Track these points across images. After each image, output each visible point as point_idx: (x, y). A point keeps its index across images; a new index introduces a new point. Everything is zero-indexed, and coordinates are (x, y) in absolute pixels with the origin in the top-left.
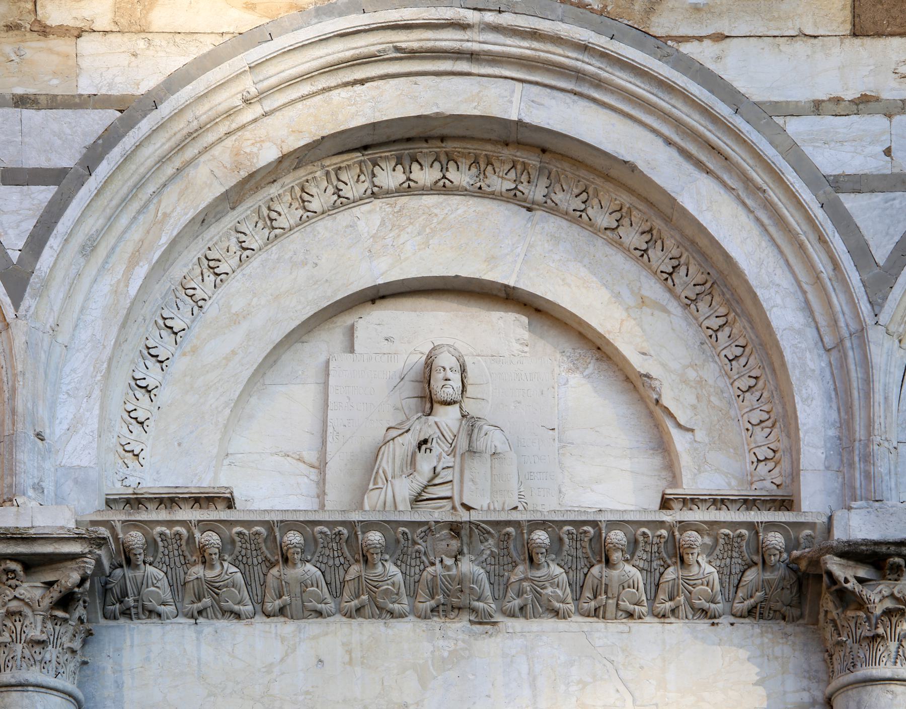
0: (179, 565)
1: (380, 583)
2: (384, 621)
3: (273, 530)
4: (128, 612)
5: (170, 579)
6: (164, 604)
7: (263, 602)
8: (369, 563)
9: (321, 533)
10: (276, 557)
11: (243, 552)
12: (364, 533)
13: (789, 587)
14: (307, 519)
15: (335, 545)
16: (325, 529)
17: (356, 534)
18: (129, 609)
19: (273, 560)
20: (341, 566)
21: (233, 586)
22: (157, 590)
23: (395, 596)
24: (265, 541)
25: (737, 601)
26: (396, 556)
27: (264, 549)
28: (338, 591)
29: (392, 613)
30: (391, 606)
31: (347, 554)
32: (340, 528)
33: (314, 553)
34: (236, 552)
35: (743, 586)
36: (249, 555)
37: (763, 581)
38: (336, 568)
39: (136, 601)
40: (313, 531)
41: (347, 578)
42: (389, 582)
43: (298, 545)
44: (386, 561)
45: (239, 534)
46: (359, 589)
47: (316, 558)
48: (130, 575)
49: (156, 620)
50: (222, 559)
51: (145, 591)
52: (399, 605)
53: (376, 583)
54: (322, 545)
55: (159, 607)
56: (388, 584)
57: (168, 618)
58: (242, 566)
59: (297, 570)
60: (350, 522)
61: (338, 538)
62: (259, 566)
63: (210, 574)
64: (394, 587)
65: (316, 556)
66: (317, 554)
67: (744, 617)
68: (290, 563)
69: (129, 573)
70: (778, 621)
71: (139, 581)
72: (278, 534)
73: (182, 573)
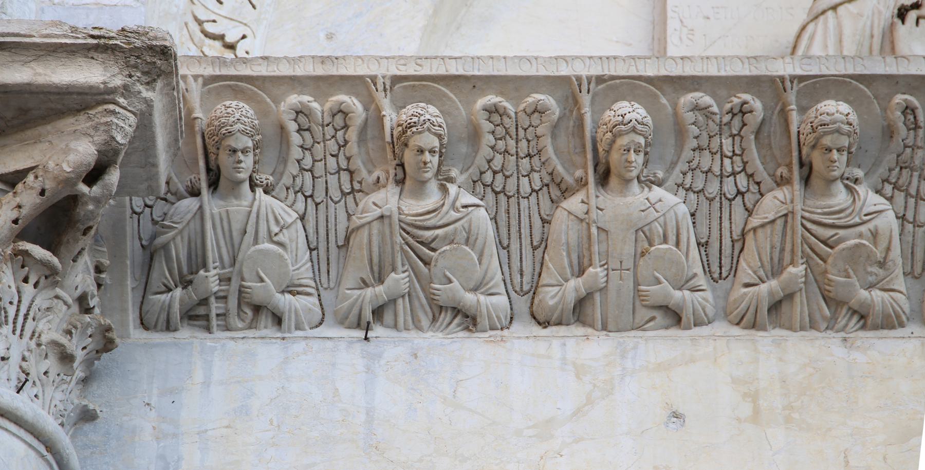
0: (336, 195)
1: (842, 232)
2: (843, 334)
3: (576, 102)
4: (201, 311)
5: (311, 231)
6: (292, 289)
7: (534, 290)
8: (814, 181)
9: (696, 108)
10: (579, 173)
11: (498, 160)
12: (803, 110)
14: (663, 72)
15: (727, 144)
16: (707, 100)
17: (784, 114)
18: (204, 302)
19: (569, 179)
20: (739, 198)
21: (467, 242)
22: (280, 250)
23: (875, 269)
24: (555, 128)
26: (882, 171)
27: (550, 150)
28: (726, 262)
29: (862, 317)
30: (864, 294)
31: (757, 164)
32: (746, 97)
33: (674, 164)
34: (481, 161)
36: (511, 168)
39: (225, 280)
40: (675, 106)
41: (755, 221)
42: (863, 229)
44: (856, 181)
45: (493, 111)
46: (782, 250)
47: (676, 176)
48: (216, 211)
49: (270, 331)
50: (444, 181)
51: (248, 250)
52: (886, 295)
53: (829, 232)
54: (694, 143)
55: (279, 296)
56: (860, 236)
57: (298, 327)
58: (490, 196)
59: (629, 199)
60: (772, 80)
61: (737, 122)
62: (533, 199)
63: (413, 207)
64: (875, 244)
66: (682, 166)
68: (613, 181)
69: (212, 205)
71: (237, 227)
72: (587, 110)
73: (342, 216)
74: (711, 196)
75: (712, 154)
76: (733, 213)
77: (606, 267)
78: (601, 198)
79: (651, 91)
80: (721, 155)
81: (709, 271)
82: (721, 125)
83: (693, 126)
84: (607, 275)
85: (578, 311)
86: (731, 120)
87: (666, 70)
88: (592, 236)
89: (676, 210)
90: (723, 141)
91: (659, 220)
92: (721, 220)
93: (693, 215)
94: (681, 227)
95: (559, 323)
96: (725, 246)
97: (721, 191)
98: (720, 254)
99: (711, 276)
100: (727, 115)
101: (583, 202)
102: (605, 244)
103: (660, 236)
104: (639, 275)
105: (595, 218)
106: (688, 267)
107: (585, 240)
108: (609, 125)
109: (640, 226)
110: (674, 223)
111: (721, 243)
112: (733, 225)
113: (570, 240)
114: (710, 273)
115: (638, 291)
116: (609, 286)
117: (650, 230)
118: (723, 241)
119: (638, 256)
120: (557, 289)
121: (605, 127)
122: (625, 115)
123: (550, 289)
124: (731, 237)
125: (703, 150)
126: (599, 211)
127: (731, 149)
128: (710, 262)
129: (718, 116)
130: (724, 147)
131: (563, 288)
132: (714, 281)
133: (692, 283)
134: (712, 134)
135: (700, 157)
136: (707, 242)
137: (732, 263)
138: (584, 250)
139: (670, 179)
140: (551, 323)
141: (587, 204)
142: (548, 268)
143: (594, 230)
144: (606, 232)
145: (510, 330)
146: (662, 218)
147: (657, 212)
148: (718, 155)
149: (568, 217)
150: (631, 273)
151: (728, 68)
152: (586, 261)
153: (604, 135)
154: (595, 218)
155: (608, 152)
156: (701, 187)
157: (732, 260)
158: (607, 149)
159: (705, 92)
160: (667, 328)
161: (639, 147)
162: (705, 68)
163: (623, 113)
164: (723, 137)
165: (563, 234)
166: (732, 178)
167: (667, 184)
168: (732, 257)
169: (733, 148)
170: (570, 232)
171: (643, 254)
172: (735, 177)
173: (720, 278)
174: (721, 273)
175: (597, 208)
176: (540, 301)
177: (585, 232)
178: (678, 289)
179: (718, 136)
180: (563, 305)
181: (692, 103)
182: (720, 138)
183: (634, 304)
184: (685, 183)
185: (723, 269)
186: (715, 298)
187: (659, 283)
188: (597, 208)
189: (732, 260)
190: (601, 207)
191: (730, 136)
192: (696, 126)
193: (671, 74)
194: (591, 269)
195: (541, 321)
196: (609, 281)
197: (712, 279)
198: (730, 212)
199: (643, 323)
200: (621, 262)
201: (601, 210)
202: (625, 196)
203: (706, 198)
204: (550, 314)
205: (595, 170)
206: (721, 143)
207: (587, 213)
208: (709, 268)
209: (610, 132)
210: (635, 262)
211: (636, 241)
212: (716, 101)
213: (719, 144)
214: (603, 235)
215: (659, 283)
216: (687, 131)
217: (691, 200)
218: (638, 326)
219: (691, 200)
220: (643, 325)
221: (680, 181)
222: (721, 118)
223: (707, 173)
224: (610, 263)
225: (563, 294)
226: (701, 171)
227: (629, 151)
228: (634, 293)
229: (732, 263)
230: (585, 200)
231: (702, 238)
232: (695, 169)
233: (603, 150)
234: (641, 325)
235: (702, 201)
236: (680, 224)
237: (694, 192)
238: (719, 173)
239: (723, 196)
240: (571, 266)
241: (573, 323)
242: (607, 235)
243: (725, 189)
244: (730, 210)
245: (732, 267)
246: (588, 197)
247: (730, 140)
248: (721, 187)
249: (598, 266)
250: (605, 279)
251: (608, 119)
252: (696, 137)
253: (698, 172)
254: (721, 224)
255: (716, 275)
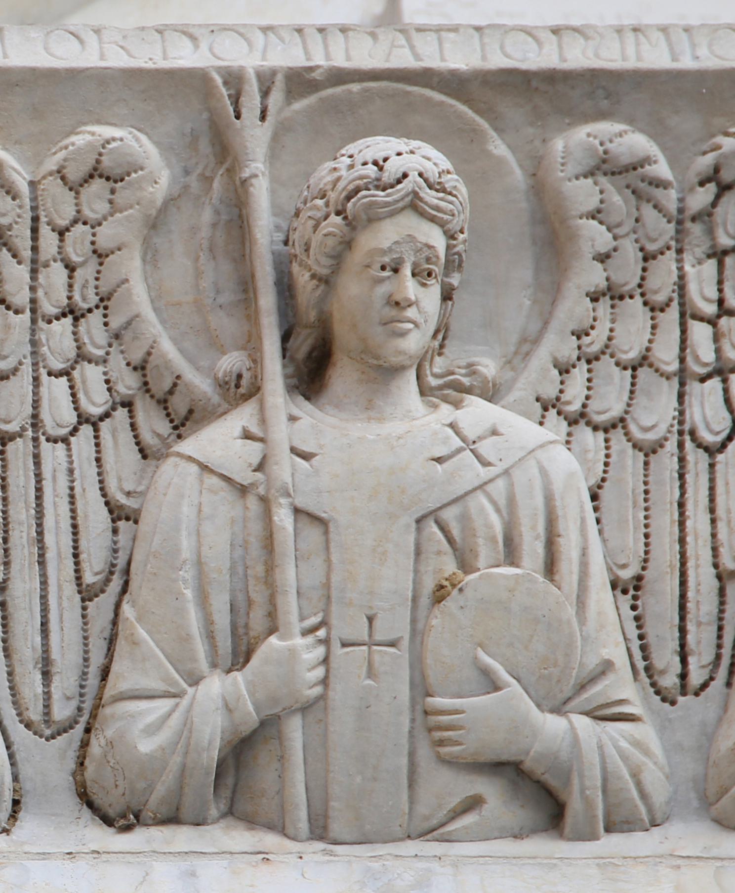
38: (696, 459)
43: (430, 196)
54: (596, 276)
59: (393, 428)
65: (542, 356)
74: (651, 436)
75: (655, 309)
76: (720, 489)
77: (321, 633)
78: (306, 421)
79: (460, 116)
80: (682, 315)
81: (647, 669)
82: (680, 222)
83: (595, 223)
84: (326, 661)
85: (230, 781)
86: (714, 204)
87: (507, 56)
88: (278, 537)
89: (545, 464)
90: (688, 268)
91: (489, 488)
92: (682, 514)
93: (594, 497)
94: (560, 513)
95: (172, 819)
96: (698, 591)
97: (681, 423)
98: (683, 618)
99: (653, 685)
100: (701, 189)
101: (247, 435)
102: (318, 562)
103: (493, 540)
104: (429, 661)
105: (289, 480)
106: (584, 639)
107: (256, 550)
108: (332, 196)
109: (432, 506)
110: (539, 501)
111: (683, 583)
112: (721, 526)
113: (205, 550)
114: (650, 677)
115: (426, 713)
116: (331, 694)
117: (465, 519)
118: (691, 573)
119: (425, 601)
120: (164, 705)
121: (320, 202)
122: (385, 160)
123: (143, 705)
124: (716, 566)
125: (621, 298)
126: (299, 460)
127: (714, 295)
128: (651, 639)
129: (673, 194)
130: (692, 288)
131: (185, 702)
132: (664, 700)
133: (596, 692)
134: (651, 247)
135: (613, 321)
136: (639, 578)
137: (719, 646)
138: (251, 582)
139: (521, 383)
140: (147, 814)
141: (262, 440)
142: (135, 643)
143: (284, 518)
144: (321, 522)
145: (13, 836)
146: (501, 483)
147: (485, 463)
148: (673, 312)
149: (202, 482)
150: (402, 654)
151: (703, 51)
152: (257, 620)
153: (316, 227)
154: (289, 480)
155: (326, 281)
156: (616, 410)
157: (720, 637)
158: (324, 271)
159: (630, 121)
160: (518, 836)
161: (428, 260)
162: (631, 51)
163: (379, 156)
164: (687, 257)
165: (184, 533)
166: (715, 383)
167: (511, 398)
168: (720, 628)
169: (720, 291)
170: (208, 528)
171: (440, 594)
172: (725, 381)
173: (684, 693)
174: (683, 676)
175: (294, 450)
176: (111, 744)
177: (256, 528)
178: (552, 711)
179: (671, 254)
180: (186, 753)
181: (591, 149)
182: (679, 261)
183: (412, 755)
184: (565, 397)
185: (691, 660)
186: (672, 748)
187: (495, 686)
188: (294, 450)
189: (720, 637)
190: (306, 448)
191: (709, 256)
192: (601, 223)
193: (524, 66)
194: (273, 640)
195: (111, 813)
196: (332, 679)
197: (657, 693)
198: (712, 489)
199: (441, 815)
200: (370, 620)
201: (306, 456)
202: (381, 420)
203: (635, 446)
204: (141, 785)
205: (285, 338)
206: (682, 277)
207: (260, 467)
208: (645, 658)
209: (338, 213)
210: (414, 621)
211: (418, 552)
212: (664, 149)
213: (675, 278)
214: (313, 534)
215: (495, 686)
216: (573, 236)
217: (587, 451)
218: (427, 825)
219: (587, 451)
220: (443, 825)
221: (550, 392)
222: (681, 200)
223: (634, 369)
224: (334, 621)
225: (187, 723)
226: (617, 364)
227: (396, 271)
228: (413, 720)
229: (719, 646)
230: (255, 430)
231: (624, 566)
232: (597, 359)
233: (313, 276)
234: (434, 822)
235: (622, 452)
236: (558, 503)
237: (596, 428)
238: (675, 366)
239: (687, 438)
240: (210, 636)
241: (216, 821)
242: (326, 532)
243: (695, 415)
244: (712, 480)
245: (718, 657)
246: (263, 421)
247: (711, 266)
248: (682, 413)
249: (297, 627)
250: (320, 672)
251: (329, 178)
252: (603, 258)
253: (606, 364)
254: (682, 524)
255: (670, 681)
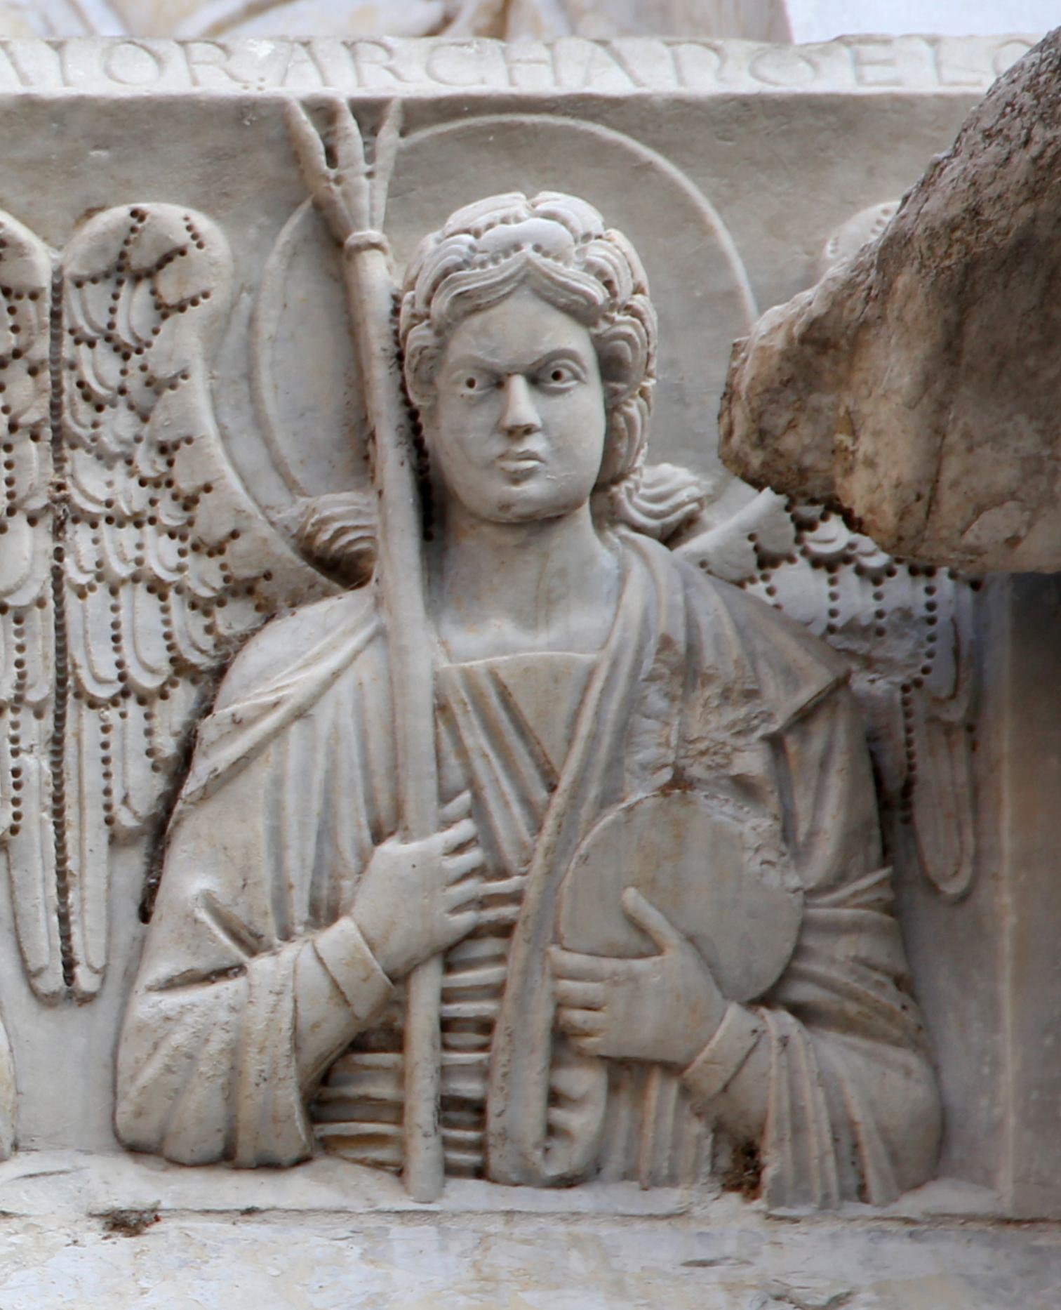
13: (752, 762)
25: (161, 967)
35: (221, 781)
37: (442, 709)
67: (269, 1165)
70: (670, 1198)
